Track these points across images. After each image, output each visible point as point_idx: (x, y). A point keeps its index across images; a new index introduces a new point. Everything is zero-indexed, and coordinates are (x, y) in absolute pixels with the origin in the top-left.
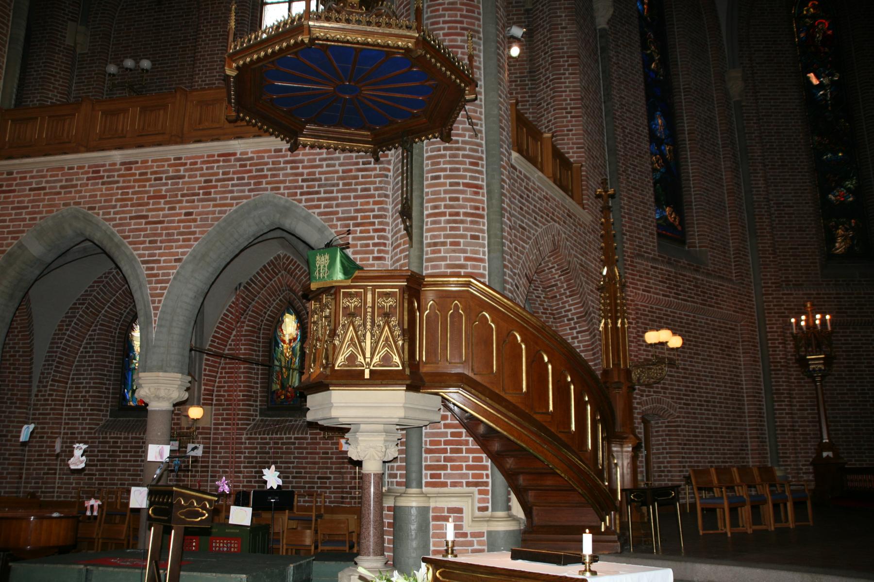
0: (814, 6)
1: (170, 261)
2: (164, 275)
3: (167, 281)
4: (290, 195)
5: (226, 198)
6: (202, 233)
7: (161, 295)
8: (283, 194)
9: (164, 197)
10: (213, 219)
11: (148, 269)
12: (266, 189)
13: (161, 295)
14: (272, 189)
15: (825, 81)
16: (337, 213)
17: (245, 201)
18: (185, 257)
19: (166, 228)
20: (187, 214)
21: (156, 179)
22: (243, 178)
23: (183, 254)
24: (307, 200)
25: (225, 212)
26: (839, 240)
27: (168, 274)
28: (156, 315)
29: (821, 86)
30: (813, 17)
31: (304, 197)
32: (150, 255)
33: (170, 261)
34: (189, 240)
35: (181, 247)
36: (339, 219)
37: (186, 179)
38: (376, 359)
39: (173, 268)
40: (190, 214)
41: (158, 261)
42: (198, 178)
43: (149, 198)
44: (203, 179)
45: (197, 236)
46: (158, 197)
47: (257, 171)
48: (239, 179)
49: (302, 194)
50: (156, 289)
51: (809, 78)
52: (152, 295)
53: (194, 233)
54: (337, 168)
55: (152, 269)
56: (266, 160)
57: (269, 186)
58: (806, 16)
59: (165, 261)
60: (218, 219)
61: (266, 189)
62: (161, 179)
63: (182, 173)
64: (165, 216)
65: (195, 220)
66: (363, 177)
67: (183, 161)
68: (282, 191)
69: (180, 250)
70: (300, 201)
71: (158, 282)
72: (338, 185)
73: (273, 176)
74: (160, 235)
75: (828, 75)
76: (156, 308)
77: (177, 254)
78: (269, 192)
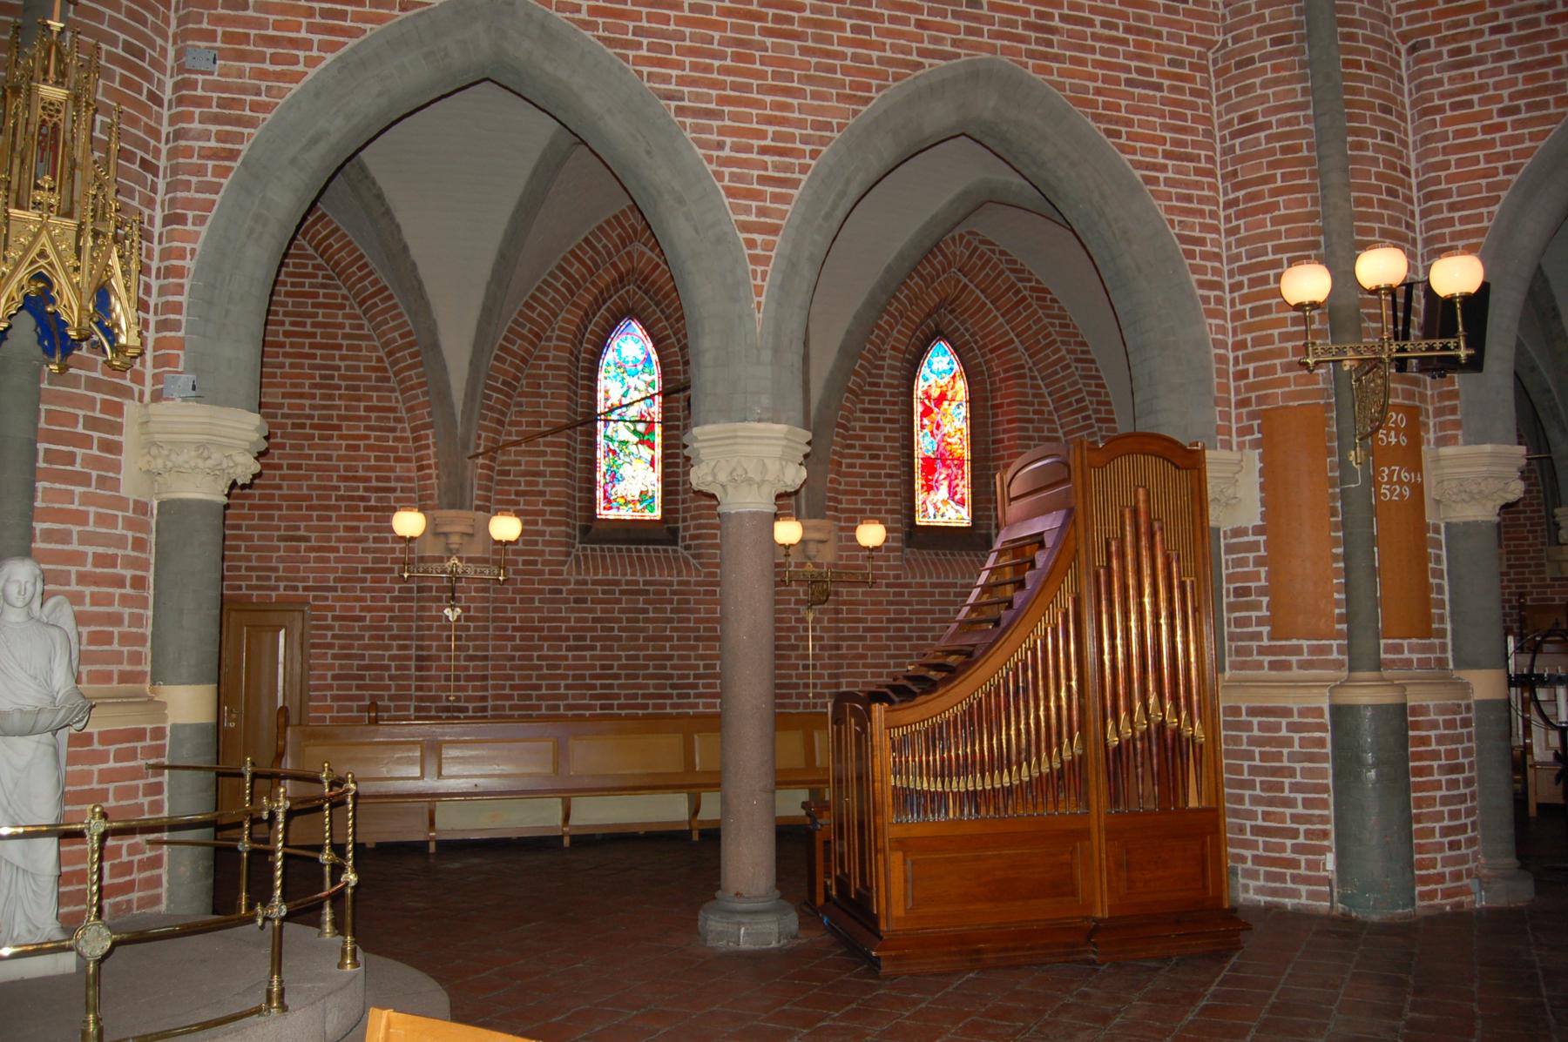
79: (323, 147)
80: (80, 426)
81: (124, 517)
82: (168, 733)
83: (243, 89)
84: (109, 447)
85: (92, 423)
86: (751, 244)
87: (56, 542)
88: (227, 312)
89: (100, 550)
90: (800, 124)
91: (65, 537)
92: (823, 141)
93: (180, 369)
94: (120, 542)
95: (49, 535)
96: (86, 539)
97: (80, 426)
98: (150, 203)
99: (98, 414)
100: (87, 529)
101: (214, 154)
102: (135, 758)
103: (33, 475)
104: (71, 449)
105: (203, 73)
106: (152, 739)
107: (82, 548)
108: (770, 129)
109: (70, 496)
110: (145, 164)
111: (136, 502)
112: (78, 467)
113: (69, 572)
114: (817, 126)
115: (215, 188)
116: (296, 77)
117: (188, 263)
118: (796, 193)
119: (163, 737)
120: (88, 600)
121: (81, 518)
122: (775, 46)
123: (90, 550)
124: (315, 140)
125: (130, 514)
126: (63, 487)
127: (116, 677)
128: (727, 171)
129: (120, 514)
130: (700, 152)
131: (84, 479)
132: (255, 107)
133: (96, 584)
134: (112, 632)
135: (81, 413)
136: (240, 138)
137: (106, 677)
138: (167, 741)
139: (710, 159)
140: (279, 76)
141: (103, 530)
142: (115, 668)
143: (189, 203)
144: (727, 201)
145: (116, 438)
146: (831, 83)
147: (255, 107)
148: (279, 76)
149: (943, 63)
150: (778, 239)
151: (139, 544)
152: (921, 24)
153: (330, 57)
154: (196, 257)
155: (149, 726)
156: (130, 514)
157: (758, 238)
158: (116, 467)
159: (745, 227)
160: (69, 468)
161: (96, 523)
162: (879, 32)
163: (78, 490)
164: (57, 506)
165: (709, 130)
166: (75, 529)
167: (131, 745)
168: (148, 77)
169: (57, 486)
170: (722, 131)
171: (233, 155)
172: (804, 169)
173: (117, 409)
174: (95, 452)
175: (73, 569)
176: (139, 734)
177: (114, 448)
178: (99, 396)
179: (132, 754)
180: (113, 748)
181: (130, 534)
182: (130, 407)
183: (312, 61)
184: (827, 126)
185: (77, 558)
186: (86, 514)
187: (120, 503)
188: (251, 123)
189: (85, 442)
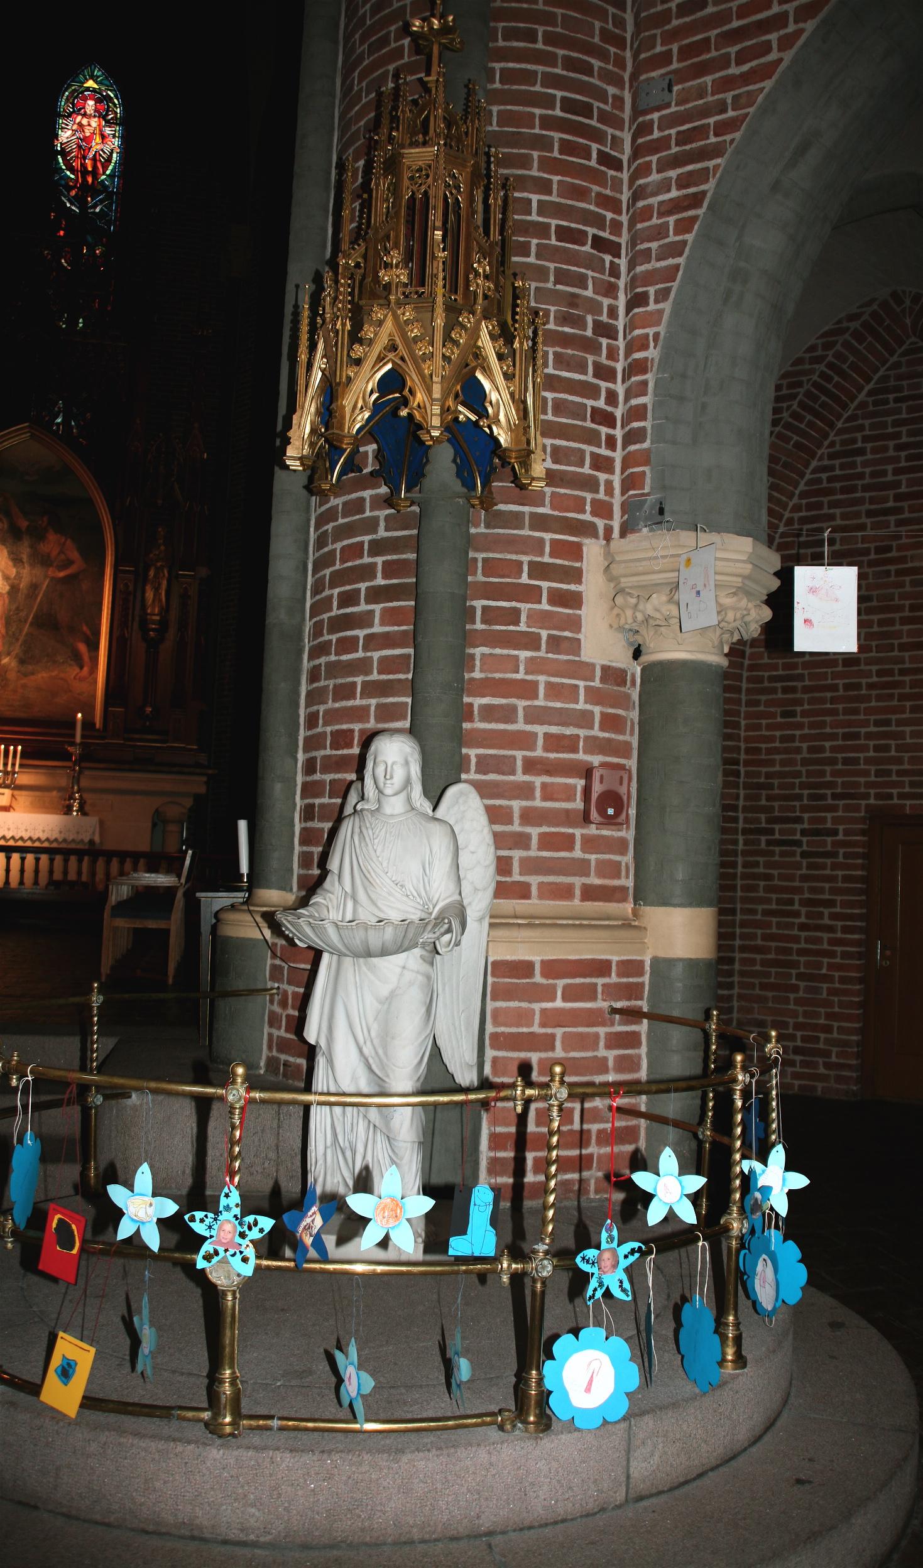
80: (525, 575)
81: (587, 688)
82: (647, 968)
84: (558, 598)
85: (539, 571)
87: (498, 721)
88: (704, 406)
89: (554, 730)
91: (508, 714)
93: (646, 491)
94: (585, 719)
95: (489, 713)
96: (534, 716)
97: (525, 575)
98: (610, 290)
99: (547, 559)
100: (536, 703)
101: (675, 207)
102: (594, 998)
103: (467, 639)
104: (514, 604)
105: (658, 109)
106: (619, 975)
107: (529, 728)
110: (599, 243)
111: (605, 669)
112: (523, 627)
113: (514, 758)
115: (676, 249)
117: (652, 353)
119: (641, 974)
120: (538, 793)
121: (528, 690)
123: (540, 730)
125: (597, 683)
126: (505, 652)
127: (578, 892)
129: (581, 684)
131: (532, 642)
133: (548, 773)
134: (573, 836)
135: (525, 559)
136: (703, 176)
137: (565, 892)
138: (646, 979)
141: (559, 705)
142: (578, 881)
143: (649, 278)
145: (573, 587)
151: (611, 723)
154: (660, 343)
155: (615, 958)
156: (597, 683)
158: (575, 624)
160: (511, 628)
161: (547, 697)
163: (524, 654)
164: (497, 676)
166: (521, 704)
167: (588, 980)
168: (597, 136)
169: (498, 651)
173: (576, 552)
174: (545, 606)
175: (519, 754)
176: (601, 968)
177: (574, 600)
178: (548, 536)
179: (590, 993)
180: (561, 983)
181: (597, 710)
182: (592, 549)
185: (525, 740)
186: (535, 684)
187: (584, 670)
188: (716, 151)
189: (532, 594)
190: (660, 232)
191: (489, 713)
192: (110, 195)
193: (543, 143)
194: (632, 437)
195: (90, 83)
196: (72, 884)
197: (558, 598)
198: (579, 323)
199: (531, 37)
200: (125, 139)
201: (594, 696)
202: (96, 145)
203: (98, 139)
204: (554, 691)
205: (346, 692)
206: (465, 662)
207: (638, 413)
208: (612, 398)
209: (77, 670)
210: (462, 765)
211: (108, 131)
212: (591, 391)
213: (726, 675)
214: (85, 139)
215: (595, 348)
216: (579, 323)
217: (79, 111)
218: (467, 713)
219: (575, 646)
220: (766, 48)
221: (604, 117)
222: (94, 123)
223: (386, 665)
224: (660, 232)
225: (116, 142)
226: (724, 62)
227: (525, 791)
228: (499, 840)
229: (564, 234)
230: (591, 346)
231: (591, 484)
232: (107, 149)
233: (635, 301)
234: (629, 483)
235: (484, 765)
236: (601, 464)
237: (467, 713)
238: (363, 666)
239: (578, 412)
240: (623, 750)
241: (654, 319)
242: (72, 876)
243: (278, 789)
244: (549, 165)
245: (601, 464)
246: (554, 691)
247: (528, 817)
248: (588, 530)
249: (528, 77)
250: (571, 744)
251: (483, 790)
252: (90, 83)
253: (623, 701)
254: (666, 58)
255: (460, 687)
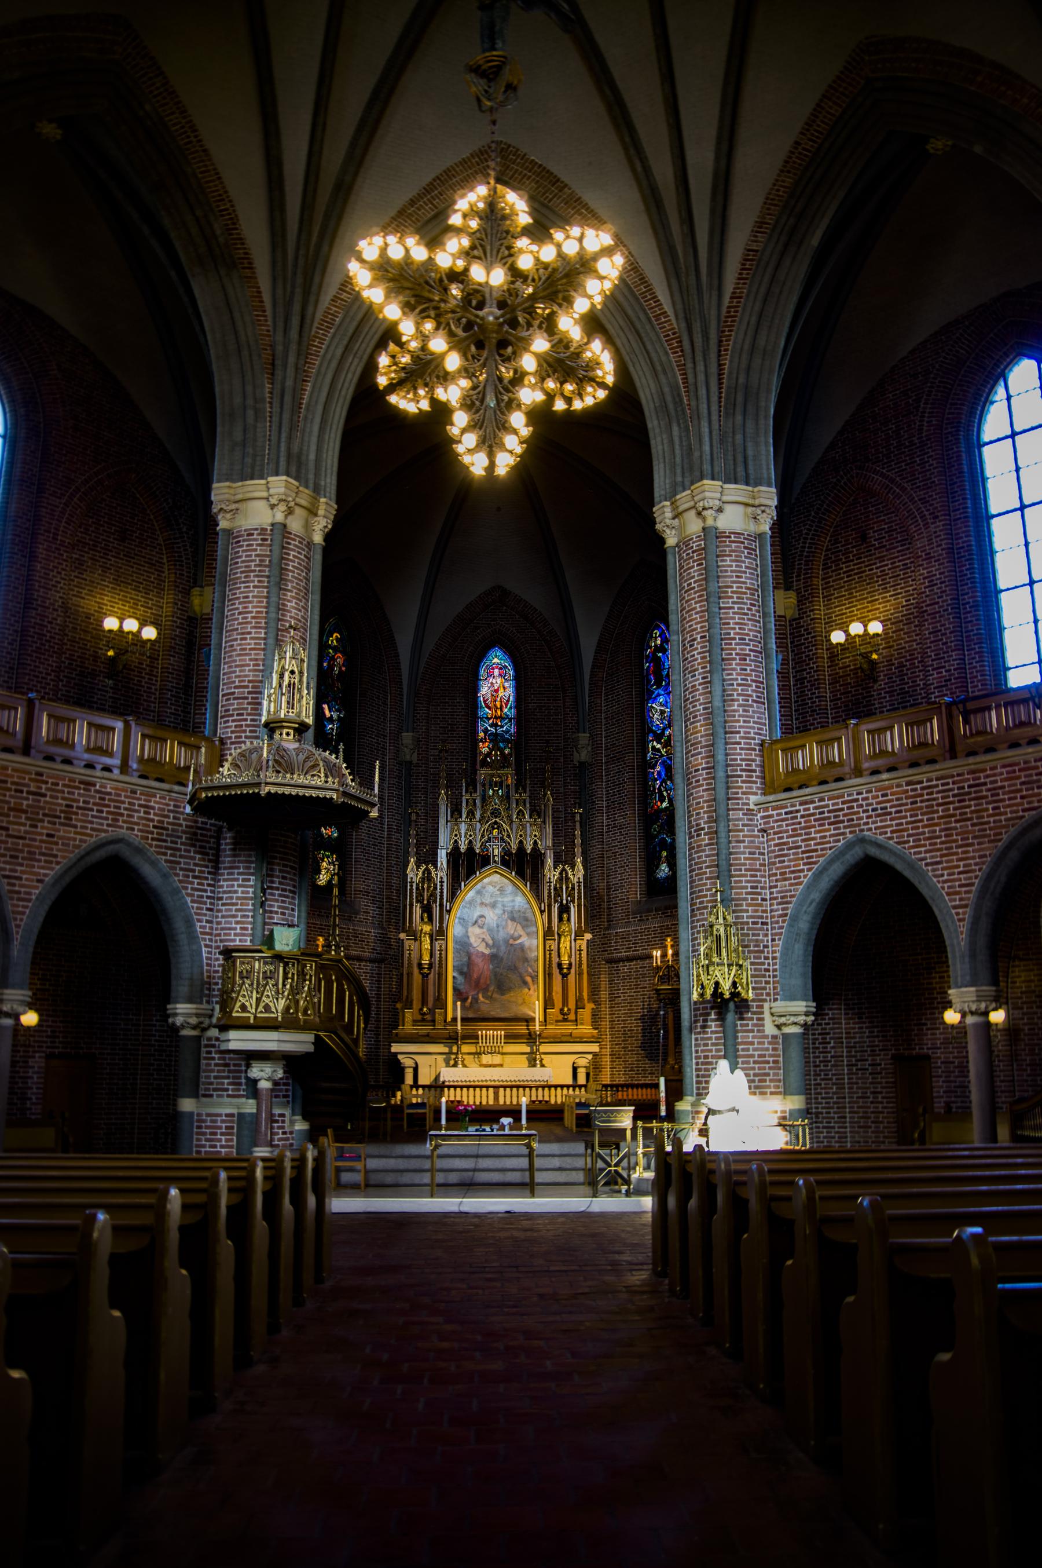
0: (337, 639)
1: (32, 881)
2: (26, 893)
3: (29, 900)
4: (142, 838)
5: (86, 828)
6: (64, 857)
7: (23, 913)
8: (137, 836)
9: (26, 812)
10: (75, 846)
11: (9, 884)
12: (121, 827)
13: (23, 913)
14: (128, 829)
15: (335, 716)
16: (179, 863)
17: (103, 835)
18: (47, 879)
19: (28, 846)
20: (48, 835)
21: (16, 791)
22: (102, 812)
23: (45, 875)
24: (157, 846)
25: (85, 841)
26: (323, 872)
27: (30, 894)
28: (17, 933)
29: (331, 718)
30: (335, 649)
31: (154, 843)
32: (11, 870)
33: (32, 881)
34: (51, 862)
35: (43, 868)
36: (181, 869)
37: (48, 799)
38: (261, 1008)
39: (37, 888)
40: (52, 836)
41: (20, 879)
42: (60, 801)
43: (10, 809)
44: (64, 803)
45: (59, 859)
46: (18, 810)
47: (115, 807)
48: (98, 811)
49: (153, 839)
50: (18, 906)
51: (323, 709)
52: (13, 912)
53: (56, 856)
54: (181, 822)
55: (14, 885)
56: (123, 798)
57: (125, 825)
58: (330, 647)
59: (27, 879)
60: (78, 847)
61: (121, 827)
62: (22, 792)
63: (43, 791)
64: (26, 832)
65: (57, 844)
66: (202, 835)
67: (44, 778)
68: (136, 832)
69: (42, 871)
70: (151, 845)
71: (19, 899)
72: (181, 838)
73: (129, 816)
74: (22, 851)
75: (337, 710)
76: (18, 926)
77: (39, 874)
78: (124, 831)
79: (814, 904)
83: (786, 891)
84: (758, 1019)
86: (958, 914)
90: (973, 858)
91: (748, 1050)
92: (983, 863)
94: (767, 1049)
95: (743, 1050)
96: (755, 1050)
98: (767, 935)
103: (737, 1032)
108: (962, 863)
109: (748, 1037)
110: (763, 923)
114: (980, 857)
115: (781, 928)
116: (800, 883)
117: (778, 955)
118: (974, 888)
121: (752, 1043)
122: (961, 827)
124: (811, 903)
128: (946, 885)
130: (935, 880)
131: (752, 1031)
132: (792, 896)
136: (787, 909)
139: (939, 882)
140: (796, 884)
143: (776, 934)
144: (947, 898)
146: (984, 836)
147: (792, 896)
148: (796, 884)
149: (1034, 812)
150: (968, 910)
151: (774, 1049)
152: (1022, 797)
153: (810, 873)
157: (960, 911)
158: (763, 1025)
159: (955, 907)
162: (1004, 807)
165: (937, 870)
168: (760, 894)
170: (942, 869)
171: (786, 915)
172: (976, 877)
173: (762, 1007)
177: (762, 1019)
182: (766, 1005)
183: (805, 876)
184: (985, 856)
185: (753, 1056)
187: (766, 1037)
190: (777, 922)
191: (743, 1050)
192: (510, 720)
193: (746, 899)
194: (775, 976)
195: (496, 660)
196: (540, 1102)
197: (758, 1019)
198: (758, 946)
199: (741, 870)
200: (518, 689)
201: (769, 1043)
202: (501, 693)
203: (501, 690)
204: (759, 1043)
205: (706, 1045)
206: (736, 1037)
207: (775, 970)
208: (769, 964)
209: (526, 990)
210: (738, 1063)
211: (506, 685)
212: (764, 964)
213: (804, 1034)
214: (497, 691)
215: (763, 952)
216: (758, 946)
217: (490, 675)
218: (738, 1050)
219: (763, 1031)
220: (800, 877)
221: (762, 888)
222: (499, 680)
223: (717, 1038)
224: (777, 922)
225: (511, 690)
226: (790, 879)
227: (753, 1069)
228: (749, 1081)
229: (753, 923)
230: (763, 952)
231: (765, 988)
232: (507, 694)
233: (773, 940)
234: (775, 988)
235: (743, 1063)
236: (767, 982)
237: (738, 1050)
238: (710, 1038)
239: (760, 970)
240: (779, 1056)
241: (778, 945)
242: (540, 1098)
243: (688, 1070)
244: (748, 905)
245: (767, 982)
246: (759, 1043)
247: (755, 1075)
248: (765, 1000)
249: (741, 882)
250: (764, 1056)
251: (743, 1069)
252: (496, 660)
253: (777, 1043)
254: (776, 875)
255: (736, 1044)
